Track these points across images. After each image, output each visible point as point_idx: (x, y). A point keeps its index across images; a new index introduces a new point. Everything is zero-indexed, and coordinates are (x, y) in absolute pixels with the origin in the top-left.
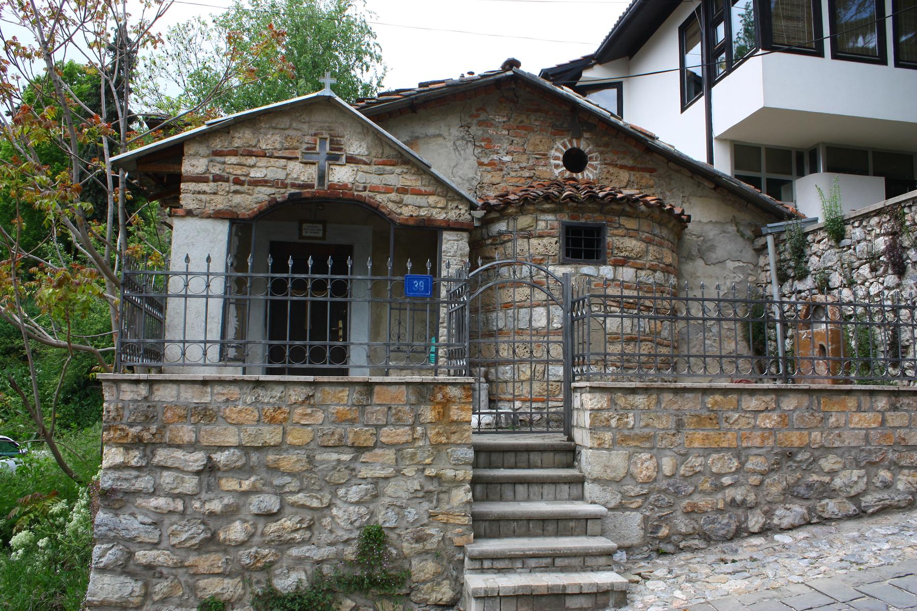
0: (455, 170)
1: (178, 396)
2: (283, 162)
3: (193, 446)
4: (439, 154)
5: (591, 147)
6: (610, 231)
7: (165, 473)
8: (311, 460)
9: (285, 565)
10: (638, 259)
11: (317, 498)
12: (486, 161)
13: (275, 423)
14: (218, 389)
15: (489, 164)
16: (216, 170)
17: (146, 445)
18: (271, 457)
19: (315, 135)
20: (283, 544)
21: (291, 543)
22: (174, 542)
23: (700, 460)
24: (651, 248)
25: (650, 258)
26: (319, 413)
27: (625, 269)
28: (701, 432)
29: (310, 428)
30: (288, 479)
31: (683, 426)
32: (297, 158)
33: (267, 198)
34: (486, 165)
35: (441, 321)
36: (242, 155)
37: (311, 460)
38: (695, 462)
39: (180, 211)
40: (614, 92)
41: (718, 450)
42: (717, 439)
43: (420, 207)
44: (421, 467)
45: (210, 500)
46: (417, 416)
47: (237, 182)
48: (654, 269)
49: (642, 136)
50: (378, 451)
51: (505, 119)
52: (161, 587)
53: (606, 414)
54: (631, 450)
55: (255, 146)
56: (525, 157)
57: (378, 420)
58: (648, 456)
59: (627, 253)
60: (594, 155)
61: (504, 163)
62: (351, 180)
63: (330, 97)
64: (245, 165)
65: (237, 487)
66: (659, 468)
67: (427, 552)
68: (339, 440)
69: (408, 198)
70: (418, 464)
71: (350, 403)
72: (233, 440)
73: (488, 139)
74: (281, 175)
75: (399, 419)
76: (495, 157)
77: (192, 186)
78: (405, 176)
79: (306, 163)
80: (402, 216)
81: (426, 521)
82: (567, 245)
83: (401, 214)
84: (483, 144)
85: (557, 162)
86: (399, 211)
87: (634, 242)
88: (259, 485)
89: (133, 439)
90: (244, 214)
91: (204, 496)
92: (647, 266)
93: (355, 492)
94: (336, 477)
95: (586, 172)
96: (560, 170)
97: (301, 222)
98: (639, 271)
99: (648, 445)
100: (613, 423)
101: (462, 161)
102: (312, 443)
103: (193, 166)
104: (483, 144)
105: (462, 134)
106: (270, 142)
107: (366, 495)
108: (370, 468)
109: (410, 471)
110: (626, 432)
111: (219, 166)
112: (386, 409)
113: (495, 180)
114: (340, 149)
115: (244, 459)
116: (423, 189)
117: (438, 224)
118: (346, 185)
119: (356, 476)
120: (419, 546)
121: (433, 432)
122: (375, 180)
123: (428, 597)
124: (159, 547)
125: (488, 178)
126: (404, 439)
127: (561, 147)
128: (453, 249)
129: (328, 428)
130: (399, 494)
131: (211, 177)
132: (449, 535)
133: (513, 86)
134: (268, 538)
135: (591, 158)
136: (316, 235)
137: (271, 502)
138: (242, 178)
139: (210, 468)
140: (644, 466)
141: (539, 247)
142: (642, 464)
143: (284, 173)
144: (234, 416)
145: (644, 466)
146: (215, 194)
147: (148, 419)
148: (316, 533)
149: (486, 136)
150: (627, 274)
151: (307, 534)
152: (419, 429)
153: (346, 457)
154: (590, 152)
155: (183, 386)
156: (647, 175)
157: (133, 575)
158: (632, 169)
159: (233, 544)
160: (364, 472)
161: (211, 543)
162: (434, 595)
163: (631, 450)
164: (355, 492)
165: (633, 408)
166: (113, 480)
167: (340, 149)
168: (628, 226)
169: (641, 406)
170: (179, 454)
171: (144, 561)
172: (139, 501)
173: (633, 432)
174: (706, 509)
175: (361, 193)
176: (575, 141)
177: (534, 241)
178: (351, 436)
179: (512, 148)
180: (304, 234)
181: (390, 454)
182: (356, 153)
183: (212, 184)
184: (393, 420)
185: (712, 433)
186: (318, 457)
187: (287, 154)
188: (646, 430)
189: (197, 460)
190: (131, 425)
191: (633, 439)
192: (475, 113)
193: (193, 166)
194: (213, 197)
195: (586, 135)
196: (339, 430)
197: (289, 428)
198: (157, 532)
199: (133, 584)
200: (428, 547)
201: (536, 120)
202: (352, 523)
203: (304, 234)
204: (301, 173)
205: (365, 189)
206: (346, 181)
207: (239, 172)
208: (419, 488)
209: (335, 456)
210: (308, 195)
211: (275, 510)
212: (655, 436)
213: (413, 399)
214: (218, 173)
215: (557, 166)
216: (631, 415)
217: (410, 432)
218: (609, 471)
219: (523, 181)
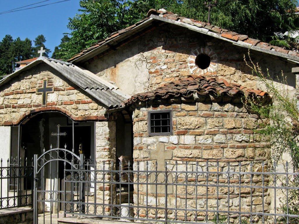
0: (136, 79)
4: (128, 71)
5: (211, 51)
6: (174, 114)
10: (197, 128)
15: (155, 72)
16: (6, 103)
19: (42, 79)
24: (209, 120)
25: (208, 127)
27: (186, 136)
32: (35, 92)
33: (24, 113)
43: (86, 110)
47: (14, 107)
49: (229, 40)
55: (19, 89)
56: (174, 64)
59: (187, 127)
60: (214, 56)
61: (163, 70)
62: (56, 100)
64: (16, 99)
69: (80, 106)
73: (154, 57)
76: (158, 67)
78: (78, 94)
84: (151, 61)
85: (192, 64)
87: (193, 119)
92: (205, 133)
95: (209, 68)
96: (193, 69)
98: (198, 137)
101: (140, 73)
104: (151, 61)
105: (140, 57)
111: (7, 100)
114: (52, 85)
116: (86, 100)
117: (92, 119)
118: (54, 103)
122: (66, 99)
138: (15, 105)
143: (30, 100)
146: (6, 113)
149: (153, 55)
150: (188, 139)
154: (211, 55)
167: (52, 85)
168: (188, 109)
179: (167, 60)
182: (58, 86)
183: (5, 109)
187: (31, 90)
192: (147, 43)
194: (5, 115)
204: (37, 99)
205: (62, 103)
206: (54, 101)
207: (14, 102)
214: (6, 104)
215: (191, 67)
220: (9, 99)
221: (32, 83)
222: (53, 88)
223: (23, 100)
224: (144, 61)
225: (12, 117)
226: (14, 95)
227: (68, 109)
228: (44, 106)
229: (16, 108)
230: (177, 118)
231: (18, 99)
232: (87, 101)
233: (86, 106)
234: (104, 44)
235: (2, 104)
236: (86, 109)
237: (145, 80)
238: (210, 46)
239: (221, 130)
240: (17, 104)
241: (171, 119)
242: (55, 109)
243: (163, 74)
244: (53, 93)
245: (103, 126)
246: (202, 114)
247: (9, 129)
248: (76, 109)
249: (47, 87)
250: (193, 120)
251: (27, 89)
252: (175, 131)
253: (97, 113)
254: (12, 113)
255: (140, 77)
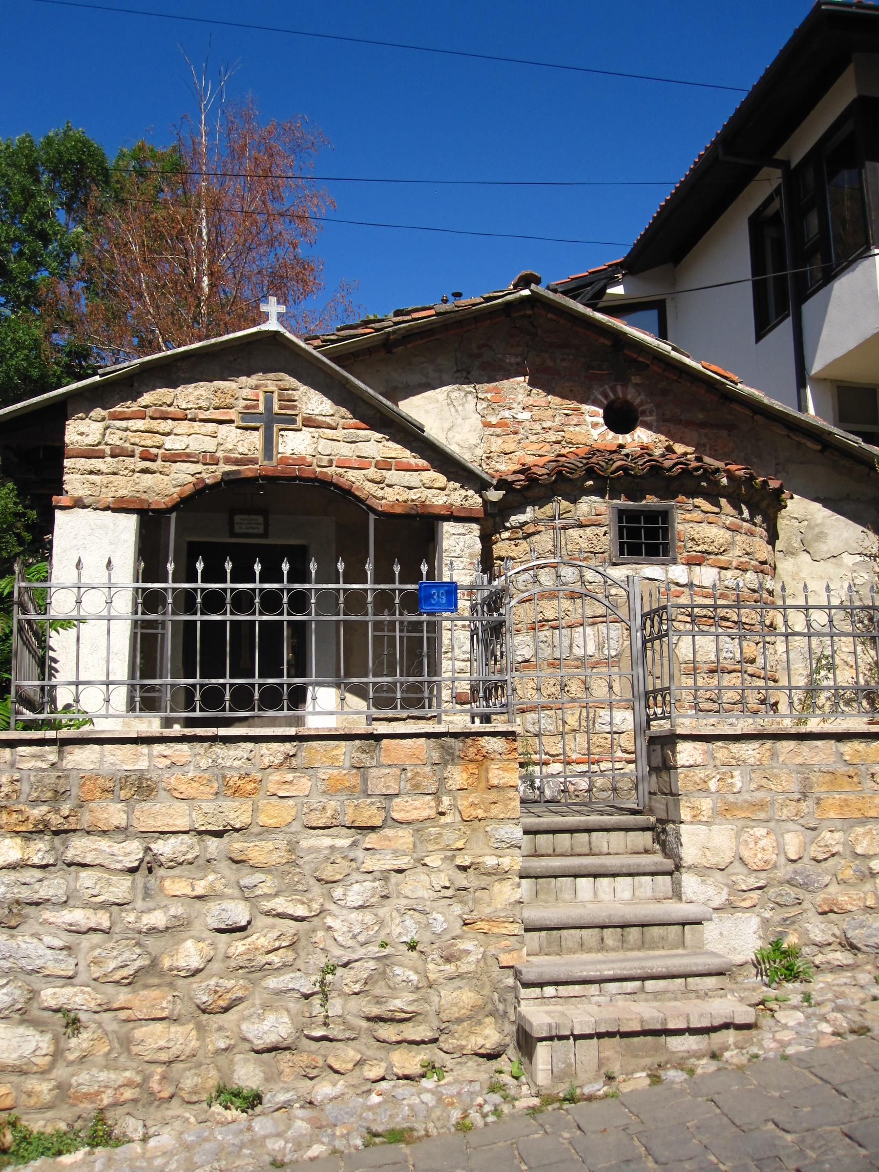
0: (450, 434)
1: (101, 761)
2: (211, 427)
3: (123, 832)
5: (643, 397)
6: (679, 516)
7: (84, 874)
8: (293, 846)
9: (257, 1002)
10: (721, 554)
11: (303, 903)
12: (494, 420)
13: (241, 795)
14: (158, 748)
15: (502, 424)
16: (114, 439)
17: (56, 833)
18: (236, 844)
20: (255, 970)
21: (266, 969)
22: (95, 975)
23: (838, 835)
24: (738, 538)
26: (304, 780)
27: (703, 568)
28: (837, 796)
29: (291, 802)
30: (259, 877)
31: (811, 787)
32: (231, 421)
33: (191, 479)
34: (494, 426)
35: (443, 650)
36: (152, 418)
37: (293, 846)
38: (833, 839)
39: (63, 500)
40: (653, 314)
41: (864, 820)
42: (861, 806)
43: (410, 488)
44: (449, 854)
45: (150, 910)
46: (443, 780)
48: (743, 569)
49: (718, 377)
50: (388, 832)
51: (519, 359)
52: (79, 1043)
53: (700, 774)
54: (740, 824)
55: (170, 406)
56: (550, 412)
57: (388, 787)
58: (763, 831)
62: (311, 451)
63: (277, 332)
65: (188, 891)
66: (780, 848)
67: (460, 976)
68: (333, 817)
69: (392, 476)
70: (447, 848)
71: (347, 764)
72: (182, 824)
74: (209, 445)
75: (416, 786)
76: (507, 414)
77: (81, 463)
79: (246, 429)
80: (384, 501)
81: (458, 932)
82: (621, 536)
83: (383, 498)
84: (489, 396)
85: (595, 419)
86: (380, 493)
88: (219, 886)
89: (35, 826)
90: (157, 502)
91: (139, 904)
92: (734, 564)
93: (356, 893)
94: (328, 873)
97: (233, 512)
99: (762, 815)
100: (713, 785)
101: (459, 421)
102: (294, 823)
103: (82, 434)
104: (489, 396)
106: (191, 398)
107: (373, 896)
108: (378, 857)
109: (433, 861)
110: (731, 798)
111: (120, 434)
112: (398, 772)
113: (509, 447)
114: (294, 407)
115: (197, 848)
117: (437, 511)
118: (303, 458)
119: (358, 869)
120: (450, 968)
121: (466, 803)
122: (345, 450)
123: (464, 1043)
124: (74, 981)
125: (497, 445)
126: (425, 814)
127: (600, 397)
128: (459, 545)
129: (315, 801)
130: (419, 894)
131: (108, 450)
132: (492, 950)
133: (529, 312)
134: (233, 964)
135: (643, 413)
136: (255, 531)
137: (239, 913)
138: (154, 451)
139: (149, 865)
140: (761, 845)
141: (580, 541)
142: (756, 843)
144: (182, 788)
145: (761, 845)
146: (115, 474)
147: (58, 795)
148: (303, 954)
150: (706, 575)
151: (290, 956)
152: (446, 800)
153: (344, 842)
154: (641, 404)
155: (108, 747)
156: (724, 433)
157: (37, 1024)
158: (703, 425)
159: (183, 974)
160: (371, 863)
161: (149, 974)
162: (473, 1039)
163: (740, 824)
164: (356, 893)
165: (740, 763)
166: (8, 885)
167: (294, 407)
169: (751, 761)
170: (104, 844)
171: (53, 1003)
172: (47, 915)
173: (740, 798)
174: (849, 907)
175: (325, 470)
176: (619, 389)
177: (574, 533)
178: (350, 810)
180: (237, 530)
181: (404, 837)
184: (408, 787)
185: (852, 797)
186: (304, 844)
188: (760, 795)
189: (131, 851)
190: (35, 803)
191: (742, 808)
193: (82, 434)
194: (112, 478)
195: (635, 380)
196: (333, 804)
197: (262, 803)
198: (72, 961)
199: (38, 1037)
200: (464, 968)
201: (563, 360)
202: (354, 937)
203: (237, 530)
205: (331, 461)
206: (304, 453)
207: (149, 443)
208: (448, 885)
209: (324, 841)
210: (250, 474)
211: (244, 923)
212: (773, 802)
213: (436, 756)
214: (118, 443)
215: (595, 425)
216: (736, 773)
217: (433, 804)
218: (708, 854)
219: (547, 447)
220: (126, 429)
221: (219, 394)
222: (299, 419)
223: (185, 438)
224: (470, 392)
225: (141, 488)
226: (148, 420)
227: (353, 479)
228: (266, 463)
229: (154, 461)
230: (687, 525)
231: (163, 434)
232: (417, 465)
233: (412, 478)
234: (390, 329)
235: (99, 443)
236: (412, 485)
237: (474, 440)
238: (637, 385)
239: (753, 562)
240: (159, 447)
241: (673, 527)
242: (312, 476)
243: (522, 431)
244: (300, 430)
245: (464, 535)
246: (728, 522)
247: (130, 522)
248: (378, 483)
249: (276, 409)
250: (715, 534)
251: (200, 408)
252: (683, 556)
253: (445, 499)
254: (138, 475)
255: (459, 430)
